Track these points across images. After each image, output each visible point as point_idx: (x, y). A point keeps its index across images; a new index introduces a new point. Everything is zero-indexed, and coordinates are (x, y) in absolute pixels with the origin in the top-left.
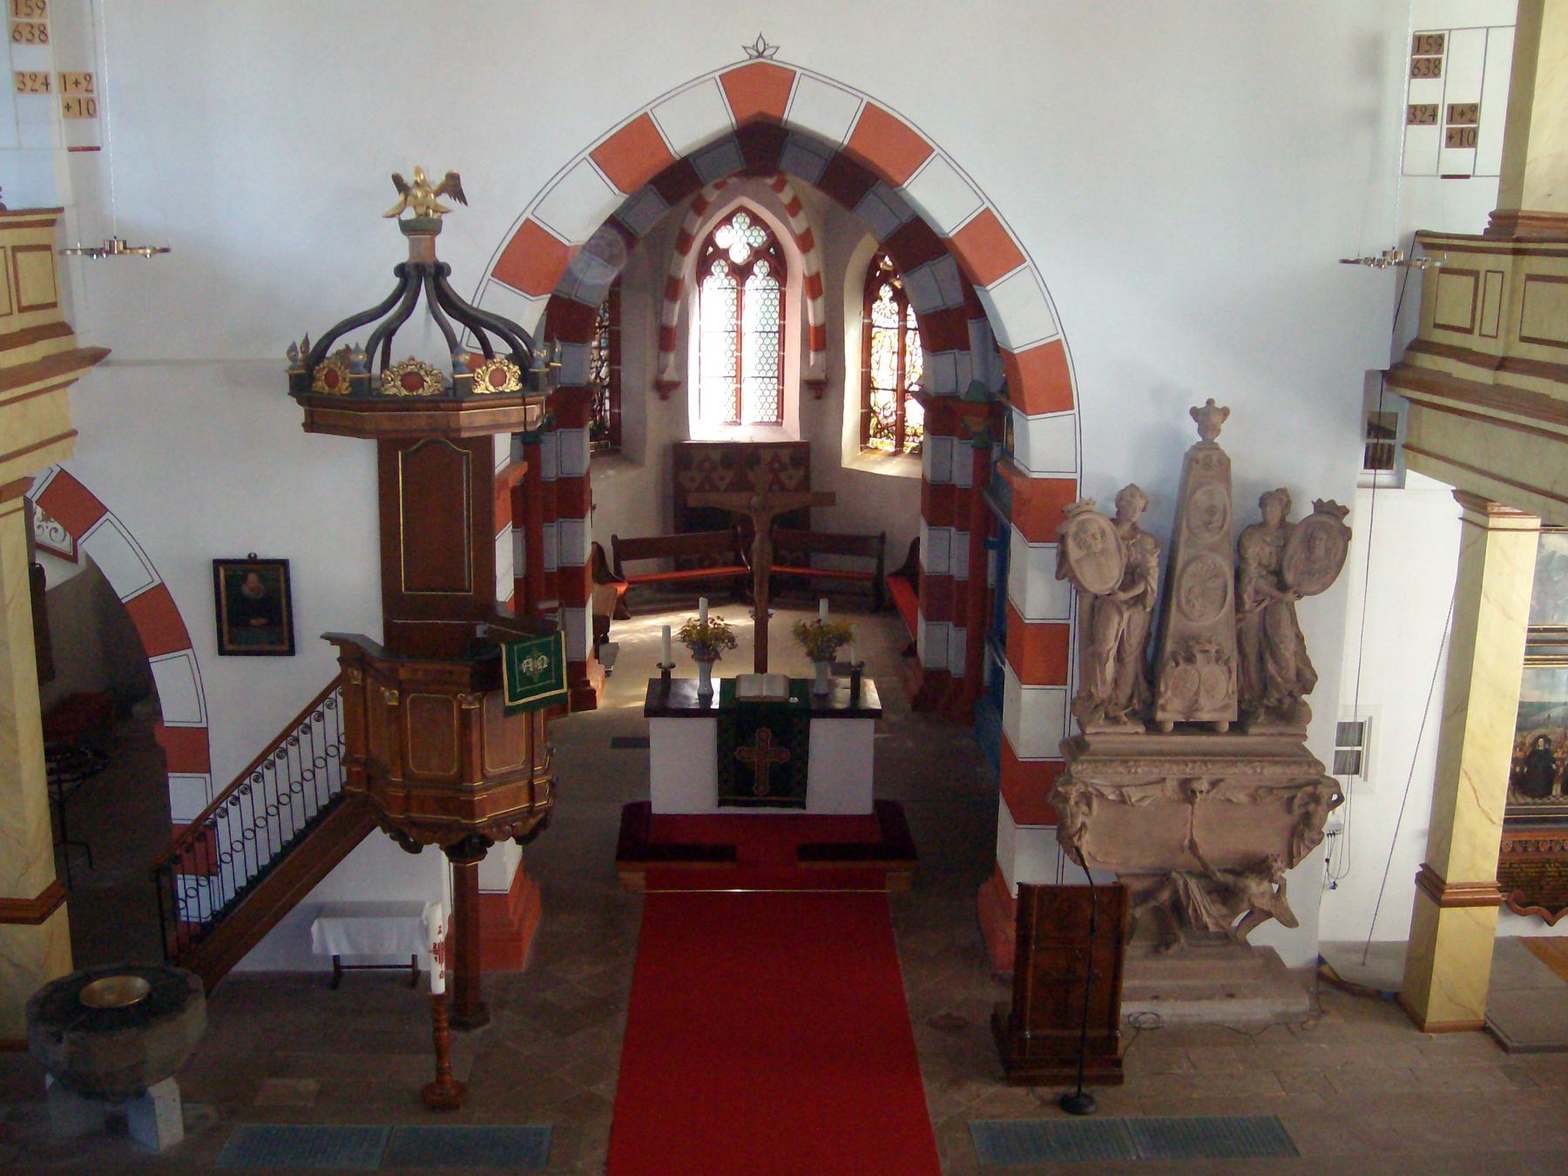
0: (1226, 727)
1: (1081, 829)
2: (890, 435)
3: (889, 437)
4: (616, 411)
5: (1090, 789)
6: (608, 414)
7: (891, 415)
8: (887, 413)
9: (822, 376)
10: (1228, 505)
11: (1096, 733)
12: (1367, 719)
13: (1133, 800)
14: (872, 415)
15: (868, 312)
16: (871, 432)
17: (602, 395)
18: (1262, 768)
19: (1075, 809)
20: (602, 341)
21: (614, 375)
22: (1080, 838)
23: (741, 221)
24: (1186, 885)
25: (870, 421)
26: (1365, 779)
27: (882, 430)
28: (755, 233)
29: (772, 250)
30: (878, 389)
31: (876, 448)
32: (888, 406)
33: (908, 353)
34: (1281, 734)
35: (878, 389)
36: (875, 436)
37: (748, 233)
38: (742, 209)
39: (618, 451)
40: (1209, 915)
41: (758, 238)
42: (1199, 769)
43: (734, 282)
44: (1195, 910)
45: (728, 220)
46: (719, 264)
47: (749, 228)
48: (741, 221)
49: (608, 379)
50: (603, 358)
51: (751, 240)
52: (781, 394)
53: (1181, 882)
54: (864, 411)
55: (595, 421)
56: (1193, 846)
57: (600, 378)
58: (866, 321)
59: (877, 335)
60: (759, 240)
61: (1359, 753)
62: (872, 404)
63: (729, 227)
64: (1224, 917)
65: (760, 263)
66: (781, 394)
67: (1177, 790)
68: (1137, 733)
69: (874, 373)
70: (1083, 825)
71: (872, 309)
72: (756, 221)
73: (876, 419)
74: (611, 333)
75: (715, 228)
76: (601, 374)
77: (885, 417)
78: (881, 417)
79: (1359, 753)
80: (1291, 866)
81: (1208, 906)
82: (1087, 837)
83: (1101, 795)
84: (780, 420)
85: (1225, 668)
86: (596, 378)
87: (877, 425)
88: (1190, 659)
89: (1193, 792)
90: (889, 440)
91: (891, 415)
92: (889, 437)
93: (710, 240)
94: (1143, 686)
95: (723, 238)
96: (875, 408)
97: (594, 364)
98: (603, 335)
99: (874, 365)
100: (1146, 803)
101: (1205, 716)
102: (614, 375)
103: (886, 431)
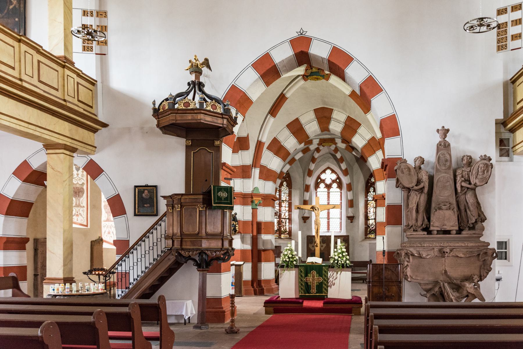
0: (455, 232)
1: (406, 266)
4: (290, 226)
5: (409, 251)
8: (373, 226)
9: (352, 215)
10: (466, 205)
11: (411, 235)
12: (508, 240)
13: (424, 256)
15: (366, 196)
18: (468, 244)
19: (404, 259)
20: (286, 205)
21: (290, 215)
22: (406, 269)
23: (328, 172)
24: (443, 284)
26: (509, 261)
27: (371, 232)
30: (370, 219)
34: (474, 234)
35: (370, 219)
38: (328, 168)
39: (291, 238)
40: (453, 295)
41: (334, 177)
42: (446, 244)
44: (447, 293)
45: (324, 171)
48: (328, 172)
52: (341, 223)
53: (442, 284)
56: (446, 272)
58: (366, 199)
61: (506, 252)
63: (325, 174)
64: (458, 297)
66: (341, 223)
67: (439, 252)
68: (424, 234)
69: (369, 215)
70: (407, 265)
72: (333, 171)
75: (320, 173)
77: (372, 228)
78: (371, 228)
79: (506, 252)
80: (481, 280)
81: (452, 293)
82: (409, 269)
83: (413, 255)
85: (453, 212)
88: (440, 209)
89: (444, 252)
93: (319, 177)
94: (426, 220)
95: (323, 177)
97: (283, 211)
99: (369, 212)
100: (428, 257)
101: (448, 228)
102: (290, 215)
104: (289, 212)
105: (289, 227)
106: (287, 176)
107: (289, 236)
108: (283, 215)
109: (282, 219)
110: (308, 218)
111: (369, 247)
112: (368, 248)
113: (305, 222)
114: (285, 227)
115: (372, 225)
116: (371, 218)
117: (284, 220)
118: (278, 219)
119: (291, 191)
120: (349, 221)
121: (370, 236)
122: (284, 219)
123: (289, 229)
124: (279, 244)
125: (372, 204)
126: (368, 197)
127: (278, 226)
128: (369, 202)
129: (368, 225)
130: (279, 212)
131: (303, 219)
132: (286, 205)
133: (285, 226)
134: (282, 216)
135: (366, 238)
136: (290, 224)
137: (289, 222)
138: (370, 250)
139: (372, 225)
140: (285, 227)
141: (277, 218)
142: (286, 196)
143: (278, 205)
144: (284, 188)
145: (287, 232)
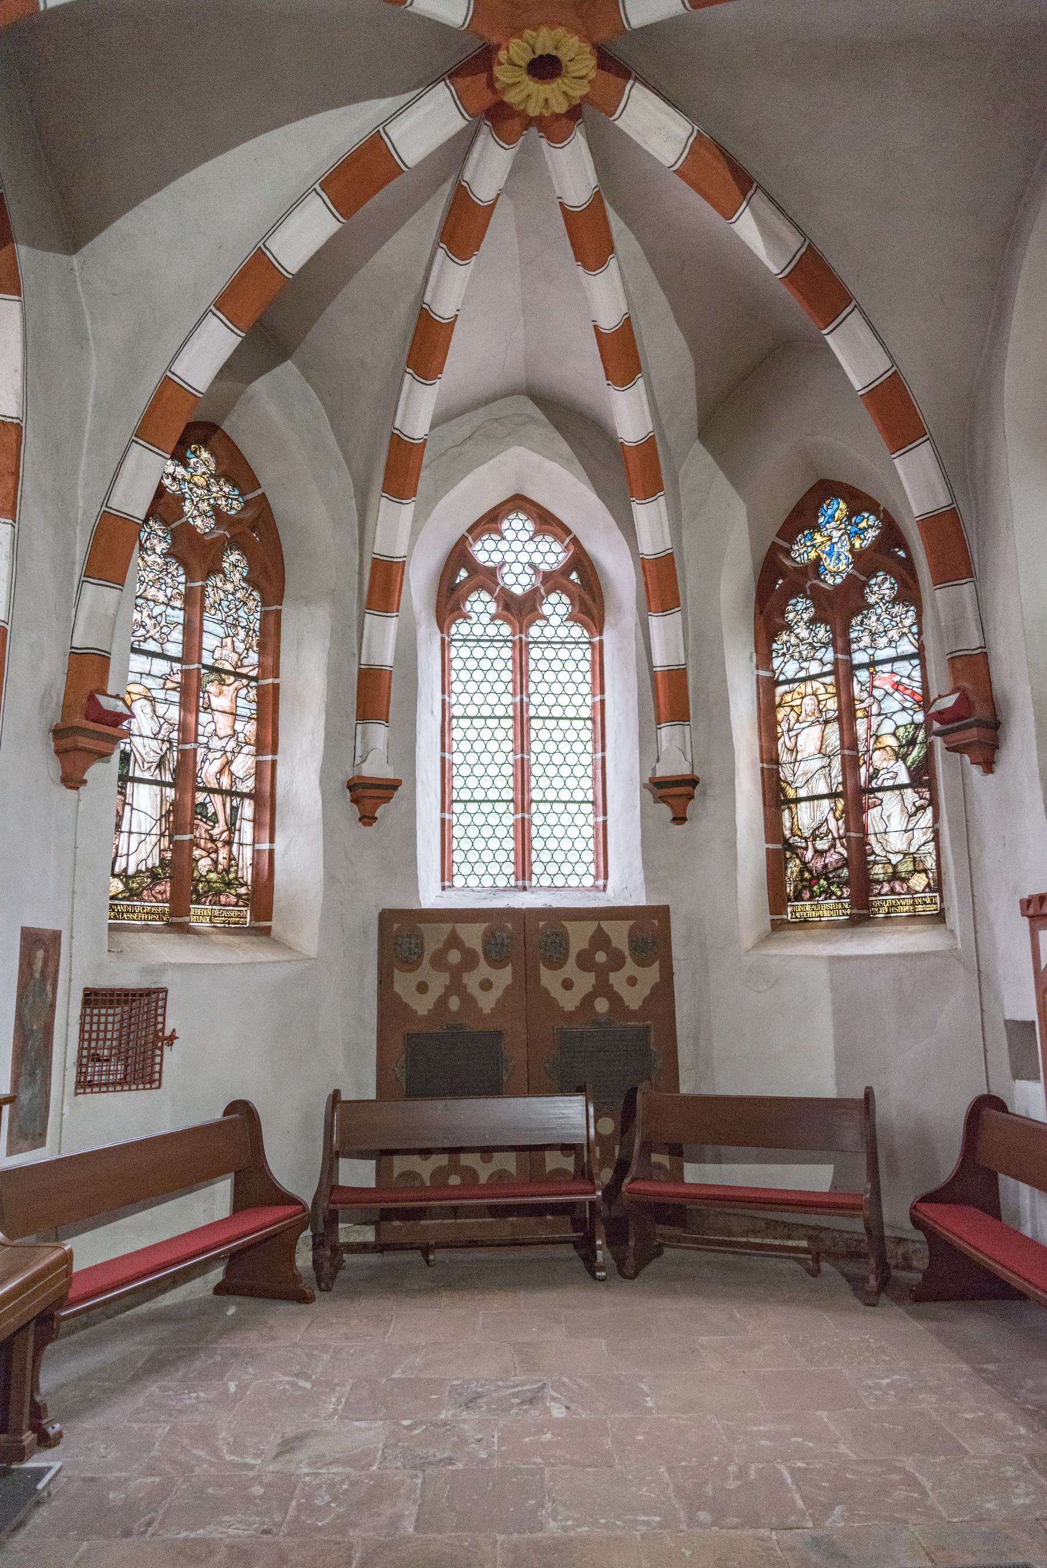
2: (833, 888)
3: (830, 894)
6: (248, 852)
7: (833, 846)
8: (822, 845)
14: (788, 854)
16: (790, 889)
17: (235, 809)
20: (241, 702)
23: (518, 526)
25: (786, 868)
28: (544, 547)
29: (574, 576)
30: (798, 800)
31: (806, 921)
32: (824, 829)
33: (859, 714)
35: (798, 800)
36: (798, 897)
37: (531, 547)
38: (518, 503)
39: (267, 931)
43: (506, 630)
46: (479, 599)
47: (531, 539)
48: (518, 526)
51: (537, 559)
52: (602, 832)
54: (771, 846)
55: (215, 862)
57: (231, 774)
58: (762, 673)
59: (788, 698)
60: (551, 558)
62: (787, 833)
65: (554, 598)
66: (602, 832)
69: (786, 773)
71: (771, 651)
73: (798, 862)
74: (261, 691)
75: (470, 530)
77: (819, 853)
84: (601, 882)
86: (221, 772)
87: (801, 872)
90: (833, 900)
91: (833, 846)
92: (833, 893)
95: (484, 552)
96: (796, 840)
98: (243, 692)
99: (785, 757)
103: (822, 882)
104: (259, 752)
105: (257, 853)
106: (249, 514)
107: (256, 917)
108: (216, 766)
109: (200, 797)
110: (388, 788)
111: (833, 990)
112: (827, 996)
113: (367, 819)
114: (223, 853)
115: (815, 836)
116: (803, 793)
117: (217, 804)
118: (170, 793)
119: (278, 613)
120: (665, 811)
121: (805, 908)
122: (217, 799)
123: (255, 865)
124: (148, 970)
125: (809, 704)
126: (776, 663)
127: (165, 842)
128: (780, 690)
129: (786, 841)
130: (183, 741)
131: (355, 800)
132: (241, 702)
133: (229, 843)
134: (209, 772)
135: (778, 926)
136: (266, 834)
137: (256, 822)
138: (837, 1011)
139: (815, 836)
140: (223, 853)
141: (162, 784)
142: (240, 647)
143: (175, 697)
144: (229, 587)
145: (243, 890)
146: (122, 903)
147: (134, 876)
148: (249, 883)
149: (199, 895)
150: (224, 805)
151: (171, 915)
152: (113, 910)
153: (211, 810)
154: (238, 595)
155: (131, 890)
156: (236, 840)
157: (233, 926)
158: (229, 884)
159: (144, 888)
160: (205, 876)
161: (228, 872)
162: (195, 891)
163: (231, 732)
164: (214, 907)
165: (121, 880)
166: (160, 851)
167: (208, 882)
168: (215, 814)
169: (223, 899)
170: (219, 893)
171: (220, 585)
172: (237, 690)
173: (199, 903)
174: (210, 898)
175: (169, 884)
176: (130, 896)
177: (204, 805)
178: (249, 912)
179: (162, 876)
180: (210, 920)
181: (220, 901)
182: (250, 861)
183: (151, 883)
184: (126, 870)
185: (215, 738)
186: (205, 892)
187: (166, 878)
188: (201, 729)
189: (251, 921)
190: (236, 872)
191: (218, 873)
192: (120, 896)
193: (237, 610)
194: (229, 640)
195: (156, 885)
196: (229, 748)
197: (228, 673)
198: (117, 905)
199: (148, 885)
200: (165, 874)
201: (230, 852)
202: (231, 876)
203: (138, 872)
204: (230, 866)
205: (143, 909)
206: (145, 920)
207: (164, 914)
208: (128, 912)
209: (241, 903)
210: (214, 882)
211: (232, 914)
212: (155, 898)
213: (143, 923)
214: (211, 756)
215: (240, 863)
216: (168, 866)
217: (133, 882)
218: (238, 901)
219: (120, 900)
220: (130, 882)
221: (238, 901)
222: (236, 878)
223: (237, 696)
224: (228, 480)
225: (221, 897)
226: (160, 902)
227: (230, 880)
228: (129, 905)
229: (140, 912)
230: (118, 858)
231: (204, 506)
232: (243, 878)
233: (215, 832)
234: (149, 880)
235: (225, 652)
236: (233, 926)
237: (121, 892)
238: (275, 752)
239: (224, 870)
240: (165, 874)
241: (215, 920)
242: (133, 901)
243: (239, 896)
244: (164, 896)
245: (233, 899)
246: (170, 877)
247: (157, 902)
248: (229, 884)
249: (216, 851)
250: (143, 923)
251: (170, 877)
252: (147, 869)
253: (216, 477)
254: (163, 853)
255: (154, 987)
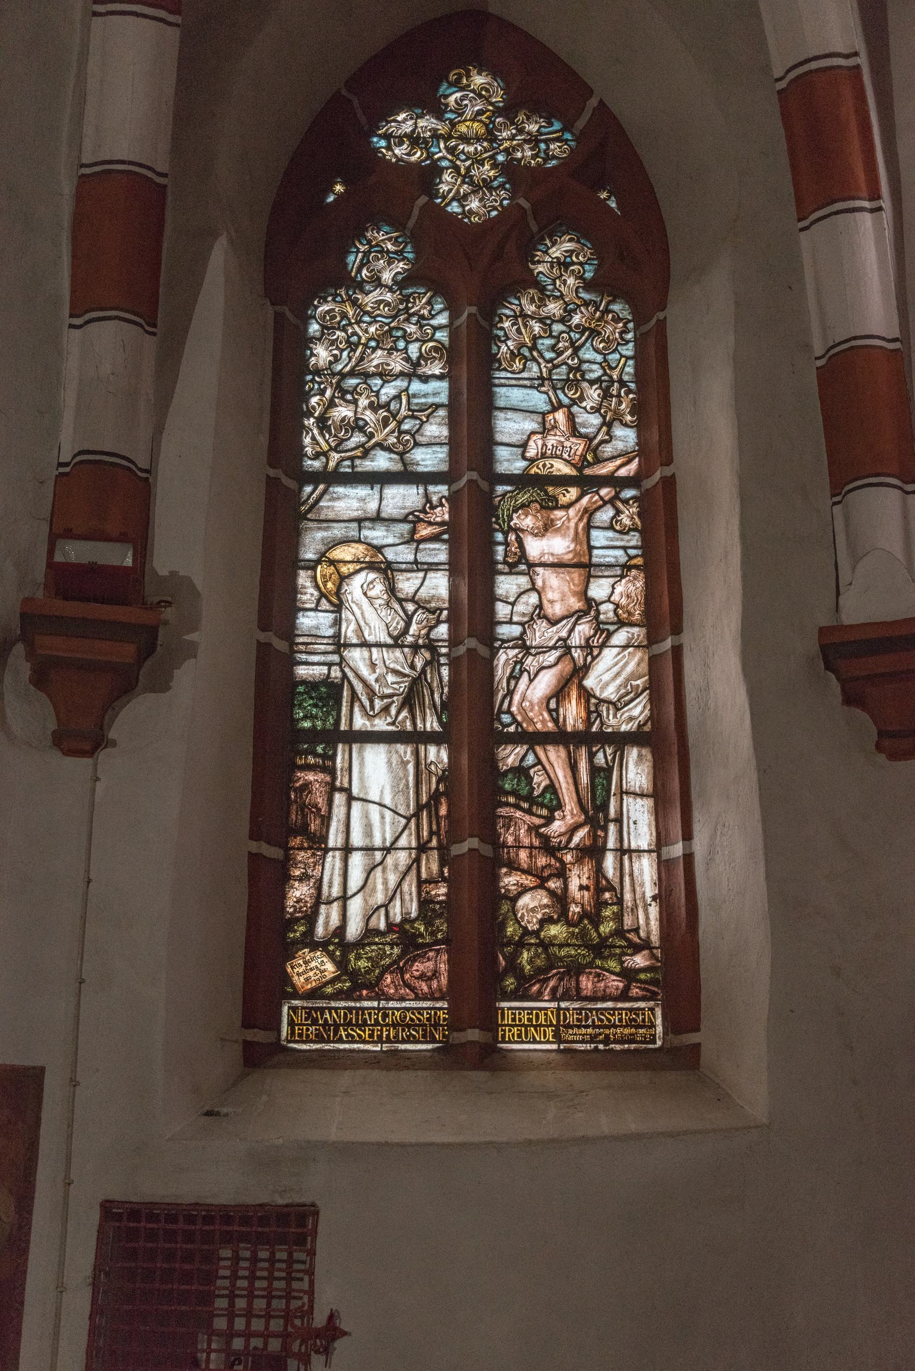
20: (599, 538)
49: (639, 710)
50: (607, 609)
55: (561, 899)
57: (586, 695)
76: (590, 682)
86: (559, 693)
104: (652, 639)
105: (664, 867)
107: (673, 1026)
108: (545, 683)
114: (578, 878)
118: (437, 755)
122: (555, 757)
123: (663, 897)
127: (431, 864)
140: (578, 878)
141: (417, 738)
142: (590, 422)
143: (439, 553)
144: (553, 308)
145: (640, 960)
146: (333, 1004)
147: (360, 944)
148: (655, 939)
149: (523, 980)
150: (573, 768)
151: (455, 1024)
152: (315, 1022)
153: (539, 780)
154: (576, 319)
155: (354, 975)
156: (611, 843)
157: (618, 1047)
158: (600, 948)
159: (385, 970)
160: (537, 933)
161: (596, 919)
162: (513, 967)
163: (576, 604)
164: (563, 1005)
165: (331, 956)
166: (420, 883)
167: (546, 945)
168: (552, 788)
169: (587, 984)
170: (575, 970)
171: (530, 309)
172: (589, 513)
173: (526, 997)
174: (552, 983)
175: (445, 957)
176: (352, 990)
177: (521, 771)
178: (659, 1012)
179: (428, 940)
180: (557, 1035)
181: (578, 988)
182: (650, 890)
183: (400, 957)
184: (341, 929)
185: (541, 626)
186: (539, 971)
187: (437, 942)
188: (502, 610)
189: (665, 1033)
190: (619, 917)
191: (569, 924)
192: (329, 990)
193: (576, 351)
194: (560, 416)
195: (414, 960)
196: (576, 640)
197: (564, 481)
198: (322, 1010)
199: (395, 962)
200: (433, 934)
201: (599, 871)
202: (606, 928)
203: (369, 933)
204: (601, 905)
205: (385, 1016)
206: (388, 1040)
207: (436, 1025)
208: (350, 1024)
209: (635, 991)
210: (561, 946)
211: (615, 1019)
212: (413, 989)
213: (386, 1047)
214: (531, 663)
215: (628, 896)
216: (440, 916)
217: (358, 958)
218: (627, 988)
219: (336, 996)
220: (352, 957)
221: (627, 988)
222: (620, 932)
223: (589, 527)
224: (536, 109)
225: (583, 979)
226: (425, 999)
227: (603, 939)
228: (350, 1009)
229: (377, 1023)
230: (323, 908)
231: (487, 171)
232: (636, 930)
233: (558, 826)
234: (396, 950)
235: (551, 441)
236: (618, 1047)
237: (332, 981)
238: (677, 630)
239: (584, 915)
240: (433, 934)
241: (570, 1034)
242: (360, 998)
243: (628, 975)
244: (435, 984)
245: (615, 983)
246: (445, 941)
247: (417, 998)
248: (600, 948)
249: (562, 873)
250: (386, 1047)
251: (445, 941)
252: (390, 926)
253: (508, 111)
254: (426, 888)
255: (280, 1201)
